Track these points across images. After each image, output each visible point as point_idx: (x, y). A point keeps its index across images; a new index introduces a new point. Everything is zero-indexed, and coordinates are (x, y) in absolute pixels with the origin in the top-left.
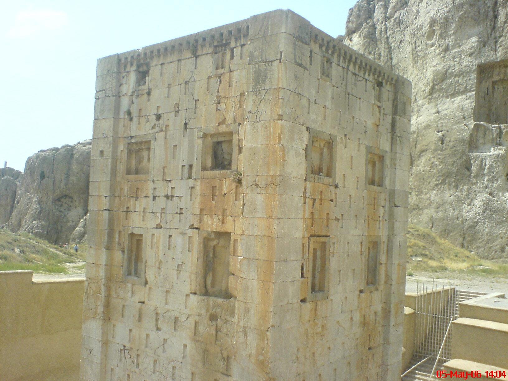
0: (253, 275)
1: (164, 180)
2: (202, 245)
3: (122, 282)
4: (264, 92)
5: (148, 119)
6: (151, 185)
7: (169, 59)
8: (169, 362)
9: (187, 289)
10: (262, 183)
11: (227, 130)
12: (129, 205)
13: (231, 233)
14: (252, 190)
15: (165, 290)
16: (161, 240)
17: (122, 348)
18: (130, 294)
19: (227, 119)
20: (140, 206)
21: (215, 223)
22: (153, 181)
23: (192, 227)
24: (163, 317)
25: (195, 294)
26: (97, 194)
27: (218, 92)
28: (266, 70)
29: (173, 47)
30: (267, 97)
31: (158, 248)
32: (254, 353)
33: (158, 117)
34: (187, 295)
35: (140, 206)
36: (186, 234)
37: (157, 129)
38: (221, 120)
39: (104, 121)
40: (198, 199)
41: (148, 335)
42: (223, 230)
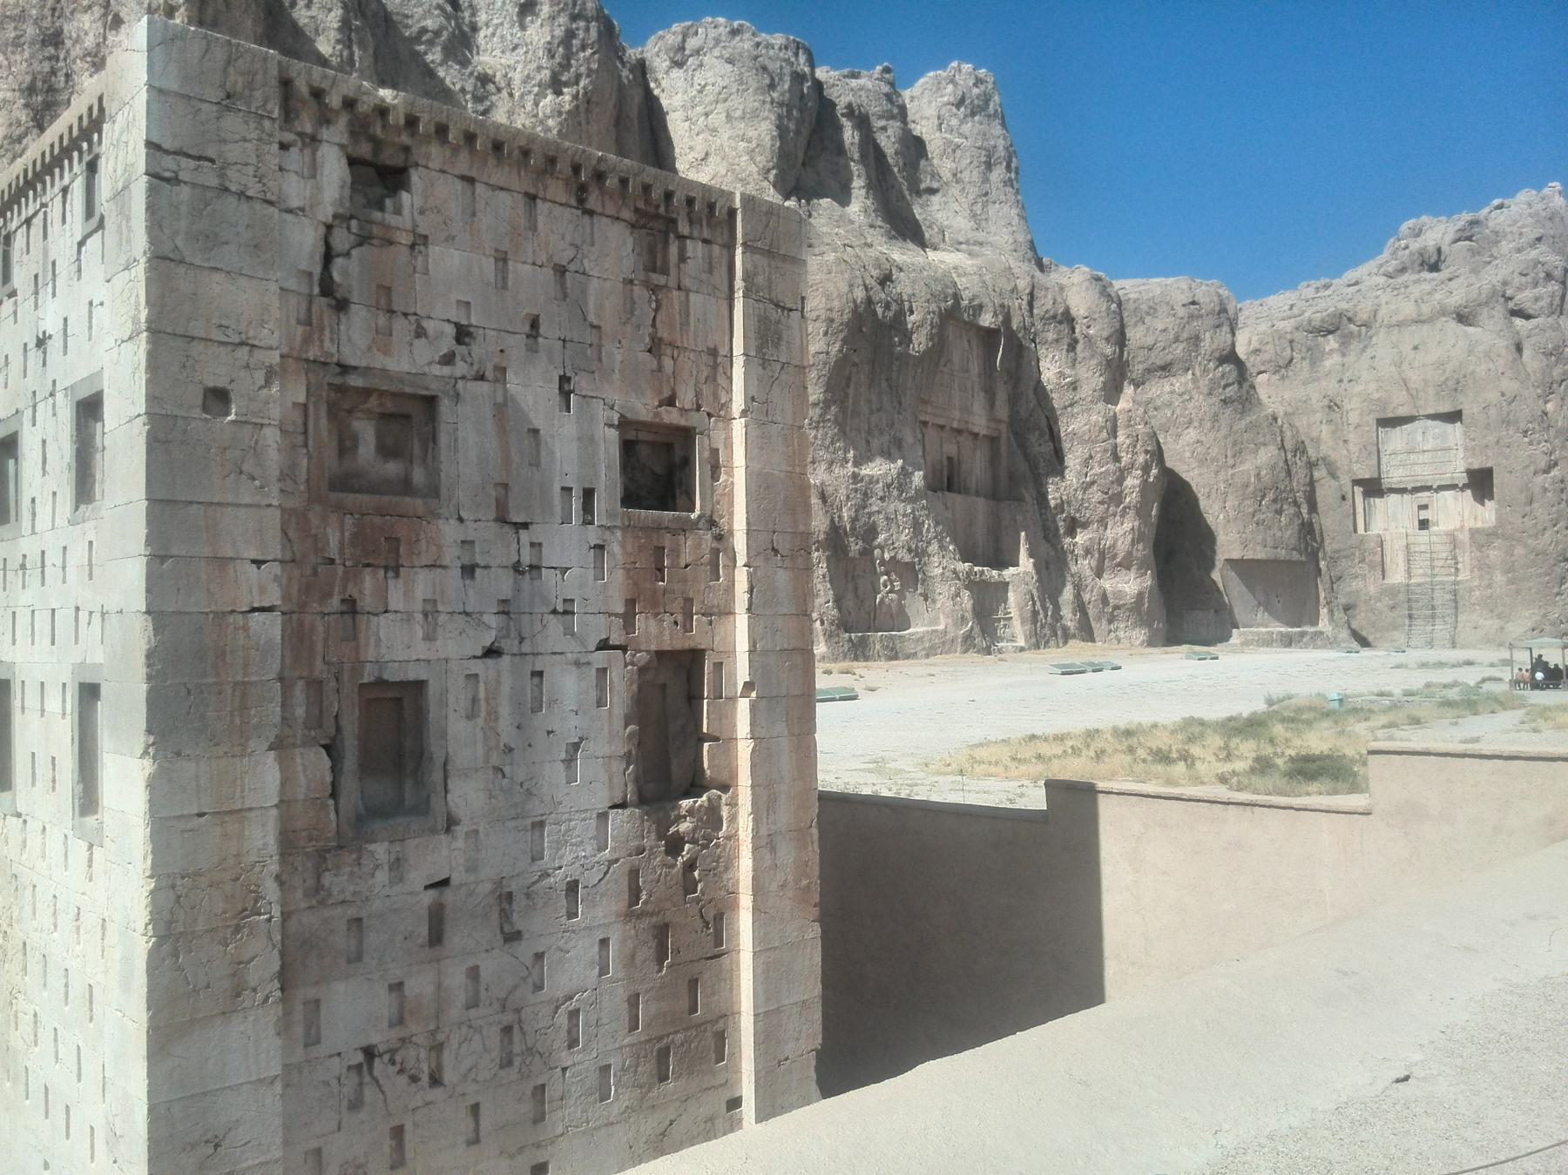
0: (781, 728)
1: (502, 519)
2: (635, 687)
3: (340, 847)
4: (779, 366)
5: (419, 326)
6: (449, 531)
7: (497, 177)
8: (557, 1008)
9: (600, 798)
10: (784, 545)
11: (683, 422)
12: (352, 590)
13: (703, 651)
14: (767, 560)
15: (529, 821)
16: (506, 689)
17: (359, 1058)
18: (382, 876)
19: (680, 394)
20: (408, 593)
21: (667, 633)
22: (461, 520)
23: (604, 645)
24: (528, 896)
25: (622, 805)
26: (207, 551)
27: (654, 325)
28: (779, 322)
29: (526, 153)
30: (783, 377)
31: (493, 715)
32: (790, 878)
33: (463, 334)
34: (603, 817)
35: (408, 593)
36: (589, 663)
37: (460, 368)
38: (666, 394)
39: (218, 277)
40: (620, 575)
41: (474, 973)
42: (687, 645)
